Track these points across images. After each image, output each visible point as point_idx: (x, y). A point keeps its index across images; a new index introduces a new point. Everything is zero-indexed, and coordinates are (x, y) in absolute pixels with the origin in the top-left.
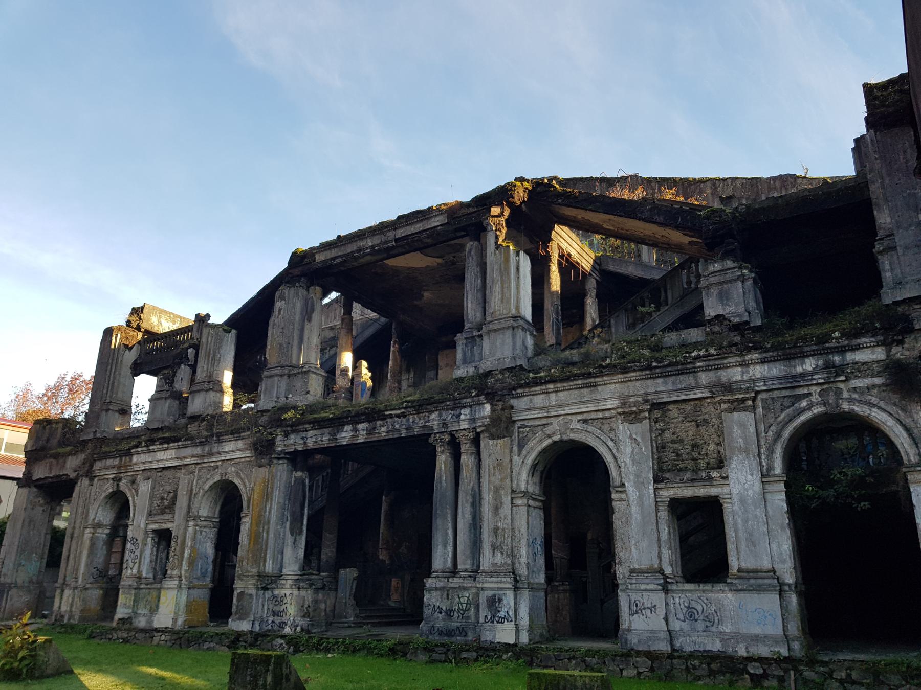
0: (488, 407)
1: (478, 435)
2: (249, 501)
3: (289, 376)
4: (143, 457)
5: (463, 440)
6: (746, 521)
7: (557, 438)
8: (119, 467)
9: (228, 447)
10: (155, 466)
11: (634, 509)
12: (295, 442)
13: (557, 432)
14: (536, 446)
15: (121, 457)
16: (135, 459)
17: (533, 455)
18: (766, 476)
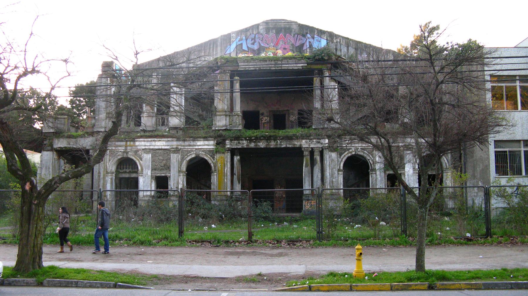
0: (327, 141)
1: (323, 149)
2: (215, 167)
3: (230, 116)
4: (143, 143)
5: (316, 151)
6: (408, 180)
7: (354, 153)
8: (126, 146)
9: (199, 143)
10: (151, 147)
11: (378, 176)
12: (235, 145)
13: (353, 151)
14: (346, 155)
15: (127, 141)
16: (137, 143)
17: (345, 158)
18: (414, 169)
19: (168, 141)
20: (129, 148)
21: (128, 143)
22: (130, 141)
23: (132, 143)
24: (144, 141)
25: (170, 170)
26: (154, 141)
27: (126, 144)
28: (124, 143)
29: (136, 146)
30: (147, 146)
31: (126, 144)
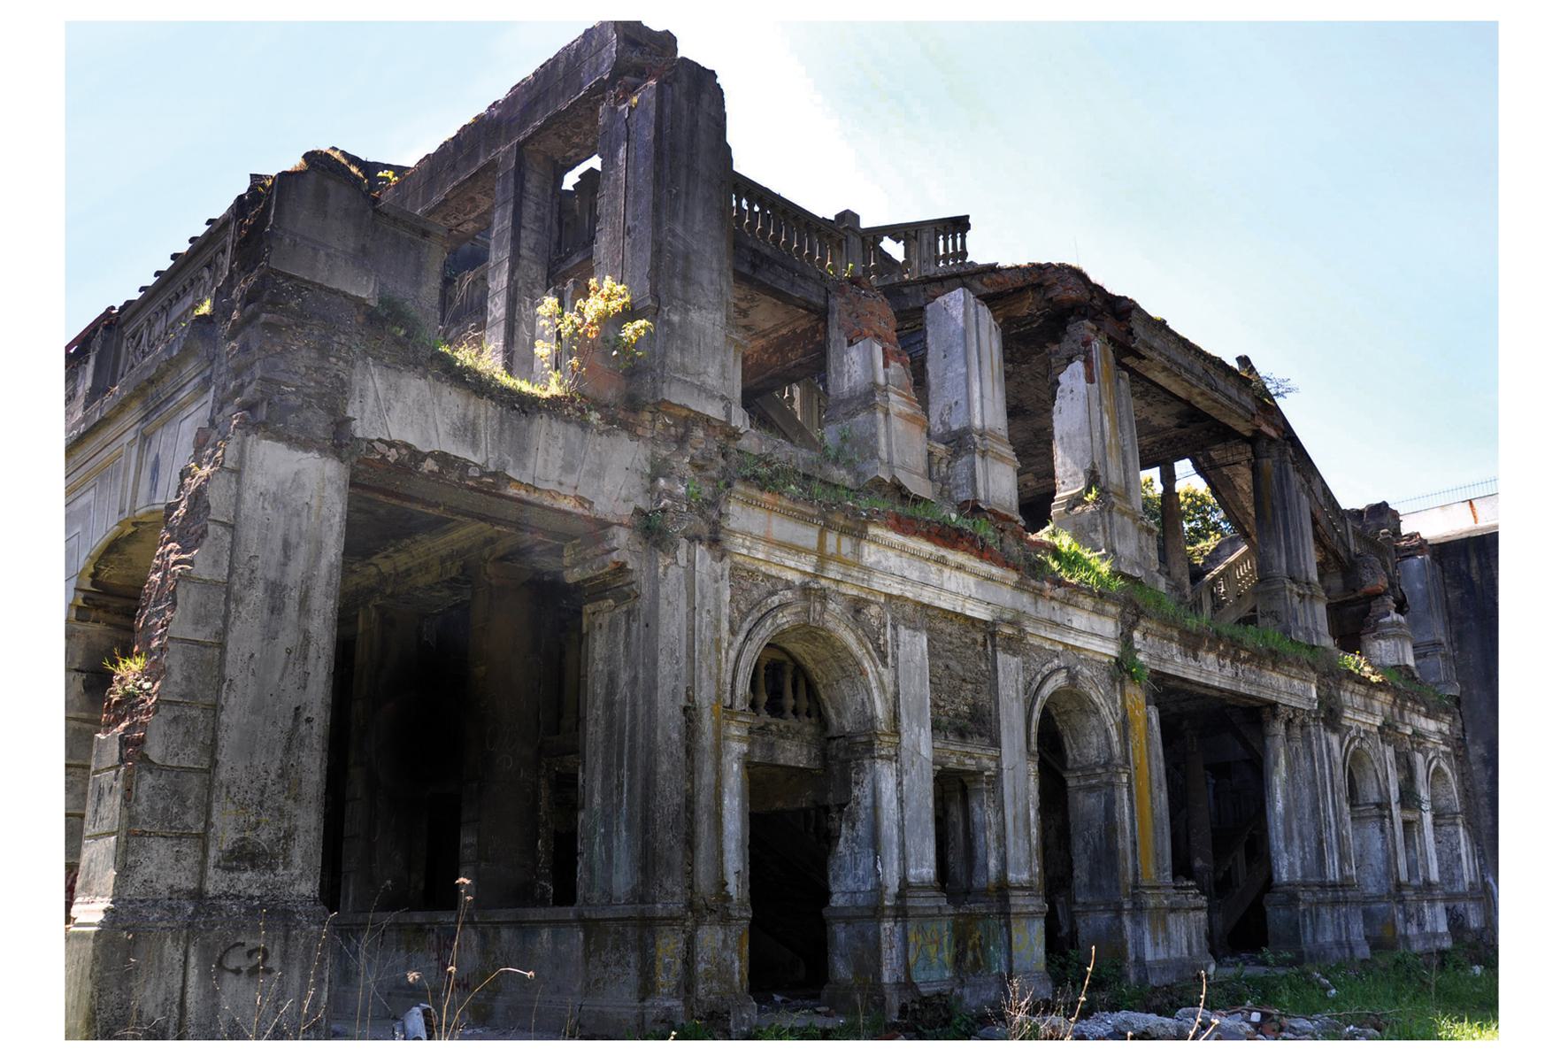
4: (893, 561)
8: (823, 558)
10: (927, 596)
15: (827, 526)
16: (870, 554)
19: (990, 578)
20: (833, 571)
21: (831, 538)
22: (843, 531)
23: (847, 545)
24: (902, 550)
25: (996, 743)
26: (942, 561)
27: (822, 543)
28: (807, 535)
29: (869, 570)
30: (914, 583)
31: (822, 543)
